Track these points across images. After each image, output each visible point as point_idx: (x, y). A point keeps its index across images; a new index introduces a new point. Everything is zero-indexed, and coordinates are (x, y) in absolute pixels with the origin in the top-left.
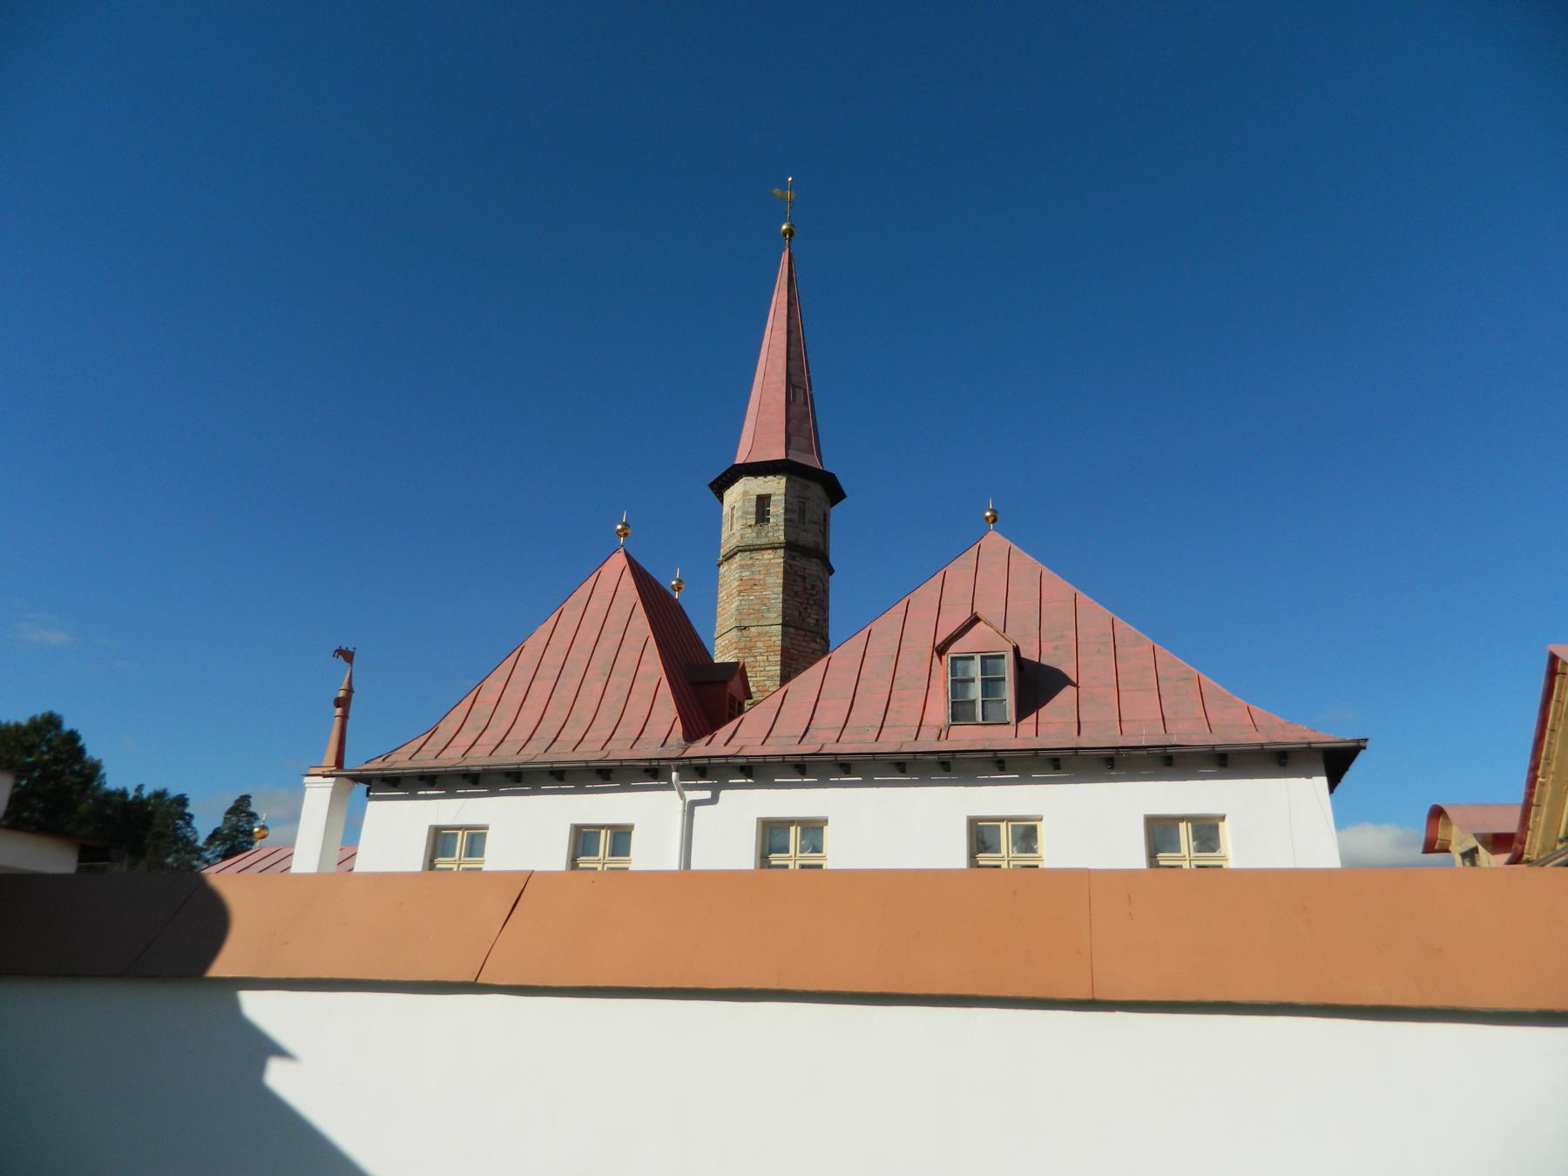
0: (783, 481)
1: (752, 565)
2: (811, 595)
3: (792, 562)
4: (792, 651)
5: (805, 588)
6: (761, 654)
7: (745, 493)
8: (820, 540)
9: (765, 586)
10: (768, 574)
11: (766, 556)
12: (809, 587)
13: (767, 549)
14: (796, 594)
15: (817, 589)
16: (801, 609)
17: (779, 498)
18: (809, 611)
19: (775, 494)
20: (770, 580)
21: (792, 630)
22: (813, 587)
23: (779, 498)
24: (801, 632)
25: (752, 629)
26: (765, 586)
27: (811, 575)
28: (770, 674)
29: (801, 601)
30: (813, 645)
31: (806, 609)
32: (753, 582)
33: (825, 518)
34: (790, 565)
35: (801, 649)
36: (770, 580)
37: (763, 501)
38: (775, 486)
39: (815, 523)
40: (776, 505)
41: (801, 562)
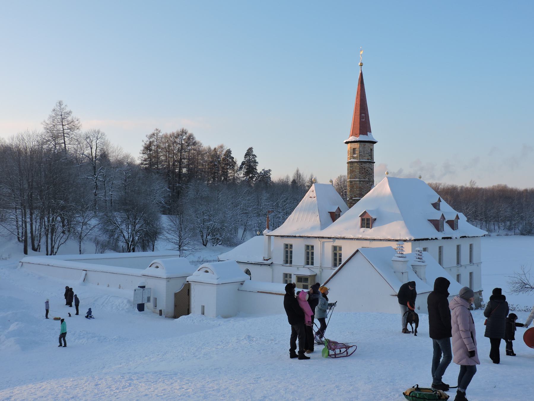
0: (359, 145)
1: (352, 166)
2: (367, 172)
3: (361, 165)
4: (362, 187)
5: (365, 171)
6: (355, 188)
7: (351, 148)
8: (369, 158)
9: (356, 172)
10: (356, 169)
11: (355, 164)
12: (366, 170)
13: (355, 163)
14: (363, 173)
15: (368, 171)
16: (364, 177)
17: (357, 149)
18: (366, 177)
19: (357, 148)
20: (357, 170)
21: (362, 182)
22: (367, 170)
23: (357, 149)
24: (364, 182)
25: (353, 182)
26: (356, 172)
27: (366, 167)
28: (357, 193)
29: (364, 174)
30: (368, 185)
31: (365, 176)
32: (352, 171)
33: (372, 150)
34: (361, 166)
35: (364, 186)
36: (357, 170)
37: (354, 149)
38: (357, 145)
39: (367, 154)
40: (357, 151)
41: (364, 165)
